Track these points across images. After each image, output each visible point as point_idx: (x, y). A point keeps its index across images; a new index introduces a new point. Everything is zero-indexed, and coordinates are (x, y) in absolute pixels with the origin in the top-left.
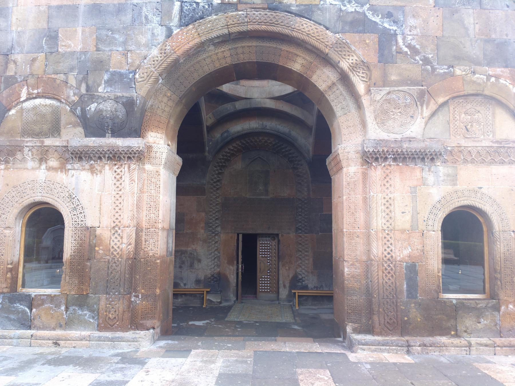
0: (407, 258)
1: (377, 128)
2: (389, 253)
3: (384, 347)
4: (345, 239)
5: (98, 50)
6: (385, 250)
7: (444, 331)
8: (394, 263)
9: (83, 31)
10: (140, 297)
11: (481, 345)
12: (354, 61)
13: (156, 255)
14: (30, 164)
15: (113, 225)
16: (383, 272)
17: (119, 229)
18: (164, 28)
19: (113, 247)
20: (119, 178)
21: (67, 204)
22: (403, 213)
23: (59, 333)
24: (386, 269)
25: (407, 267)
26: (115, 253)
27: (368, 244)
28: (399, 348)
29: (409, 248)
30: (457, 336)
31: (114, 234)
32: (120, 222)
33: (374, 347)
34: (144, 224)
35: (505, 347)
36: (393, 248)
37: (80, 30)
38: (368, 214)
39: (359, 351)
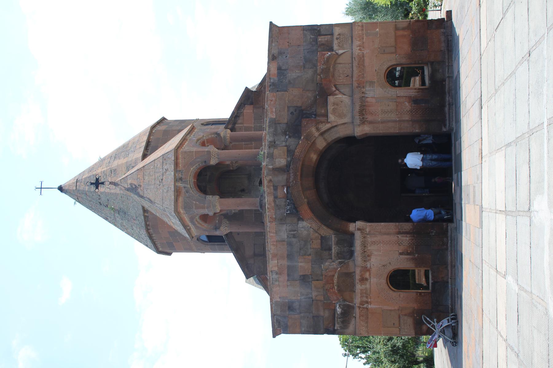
0: (410, 104)
1: (347, 118)
2: (408, 112)
3: (451, 115)
4: (402, 131)
5: (310, 255)
6: (407, 114)
7: (444, 86)
8: (412, 110)
9: (301, 262)
10: (432, 231)
11: (448, 71)
12: (315, 130)
13: (412, 225)
14: (368, 286)
15: (397, 245)
16: (417, 115)
17: (399, 241)
18: (299, 222)
19: (408, 244)
20: (374, 243)
21: (388, 267)
22: (388, 106)
23: (449, 268)
24: (416, 113)
25: (414, 104)
26: (411, 243)
27: (404, 121)
28: (451, 109)
29: (405, 103)
30: (445, 81)
31: (402, 244)
32: (396, 241)
33: (451, 120)
34: (398, 230)
35: (449, 61)
36: (405, 110)
37: (300, 264)
38: (389, 121)
39: (453, 126)
